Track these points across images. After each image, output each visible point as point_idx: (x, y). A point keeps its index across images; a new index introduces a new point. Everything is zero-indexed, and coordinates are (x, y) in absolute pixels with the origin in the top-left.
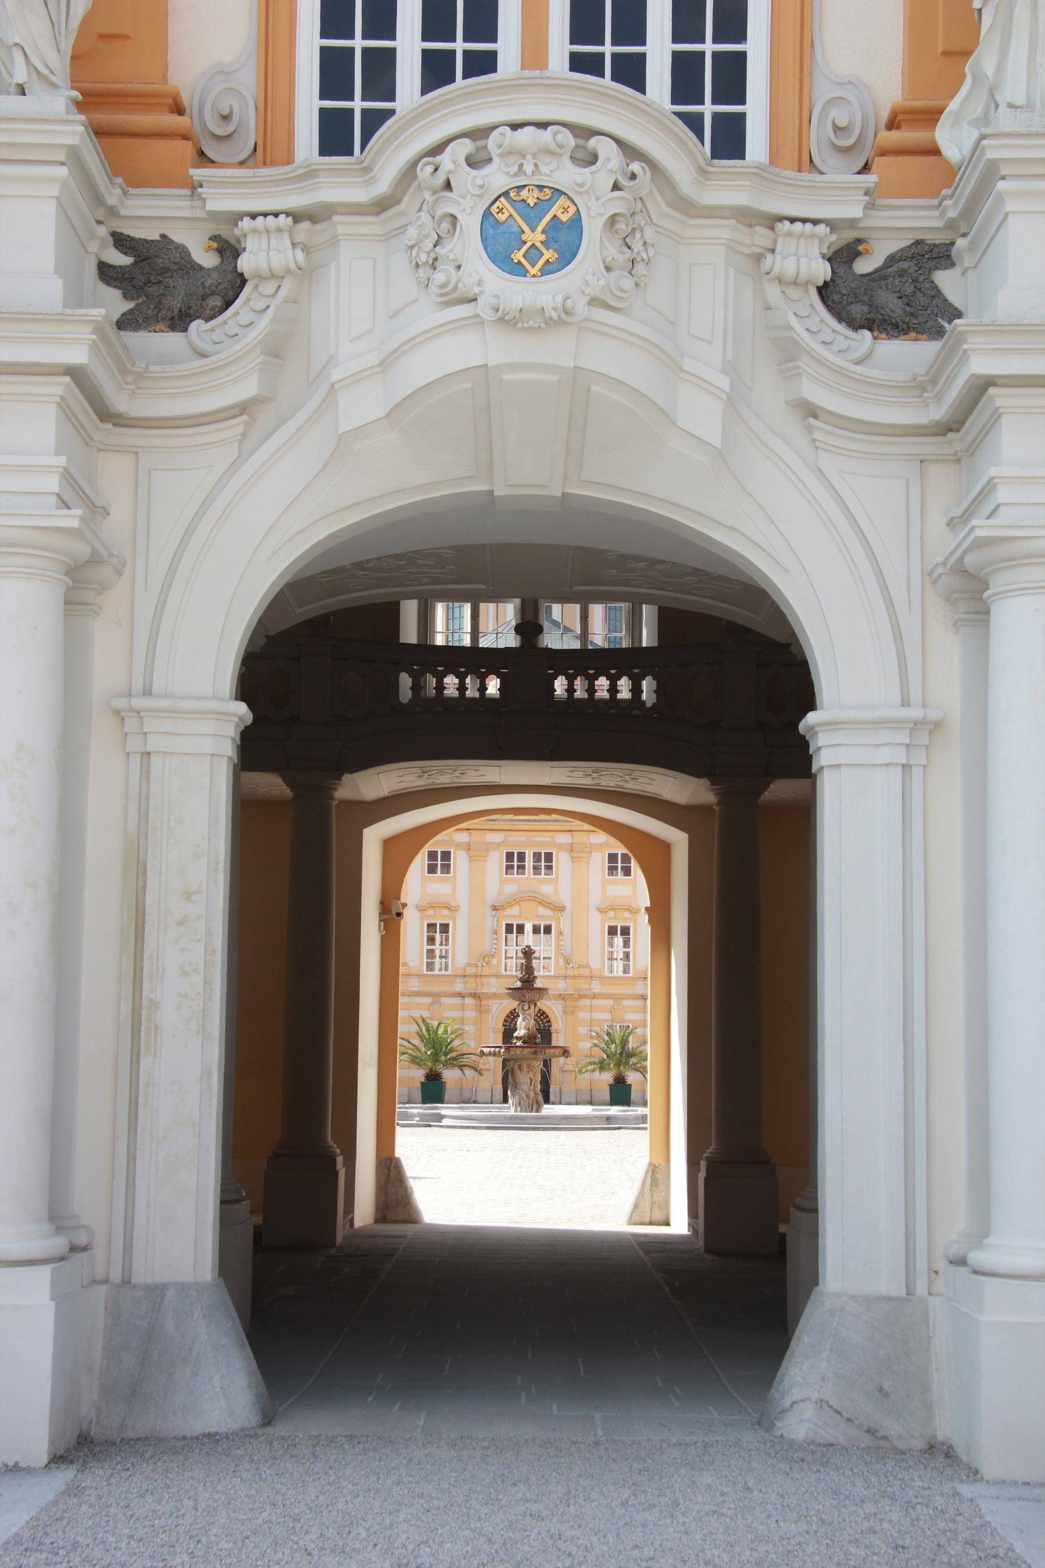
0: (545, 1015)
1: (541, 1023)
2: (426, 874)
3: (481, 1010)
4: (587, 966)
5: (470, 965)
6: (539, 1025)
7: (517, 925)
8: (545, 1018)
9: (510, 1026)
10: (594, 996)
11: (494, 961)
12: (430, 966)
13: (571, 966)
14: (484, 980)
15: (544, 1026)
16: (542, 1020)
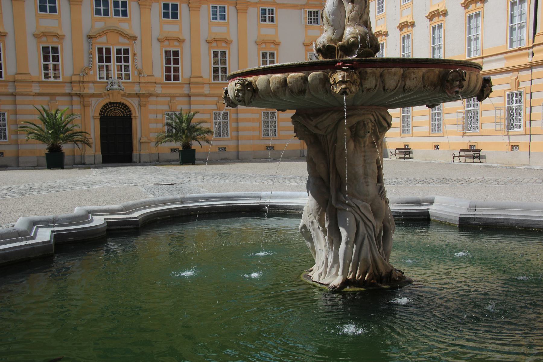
0: (127, 108)
1: (124, 112)
2: (39, 12)
3: (84, 105)
4: (153, 76)
5: (74, 75)
6: (123, 114)
7: (106, 49)
8: (127, 109)
9: (104, 114)
10: (157, 95)
11: (91, 73)
12: (47, 76)
13: (142, 76)
14: (85, 84)
15: (127, 114)
16: (125, 111)
